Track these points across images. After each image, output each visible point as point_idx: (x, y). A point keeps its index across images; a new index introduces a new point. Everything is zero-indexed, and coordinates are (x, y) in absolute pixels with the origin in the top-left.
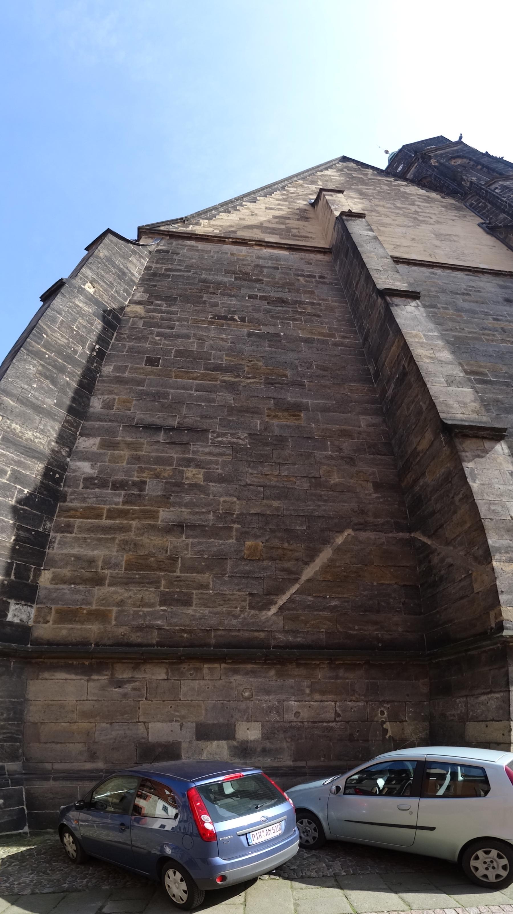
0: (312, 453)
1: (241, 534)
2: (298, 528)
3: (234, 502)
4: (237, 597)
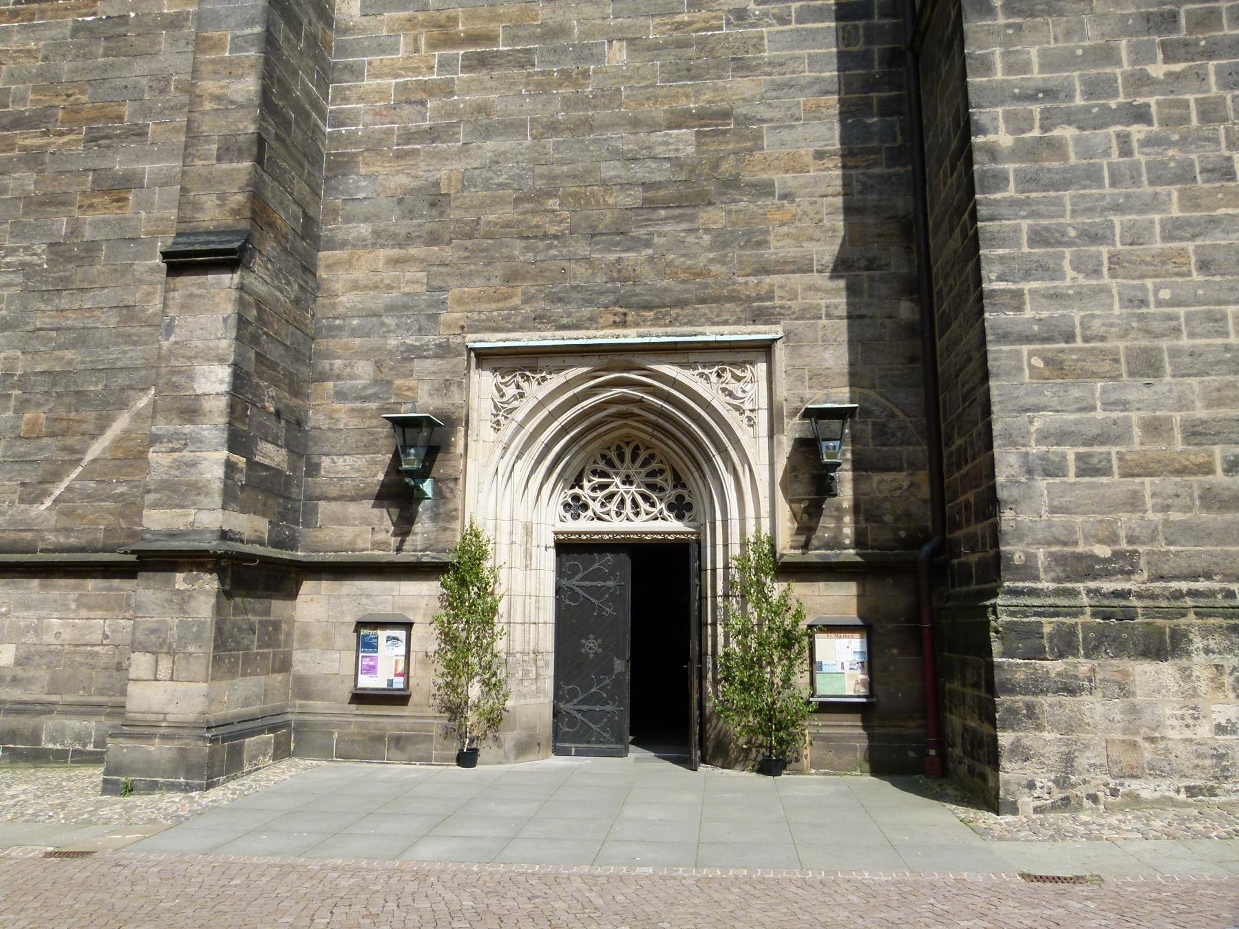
0: (131, 265)
1: (22, 402)
2: (92, 388)
3: (17, 358)
4: (6, 488)
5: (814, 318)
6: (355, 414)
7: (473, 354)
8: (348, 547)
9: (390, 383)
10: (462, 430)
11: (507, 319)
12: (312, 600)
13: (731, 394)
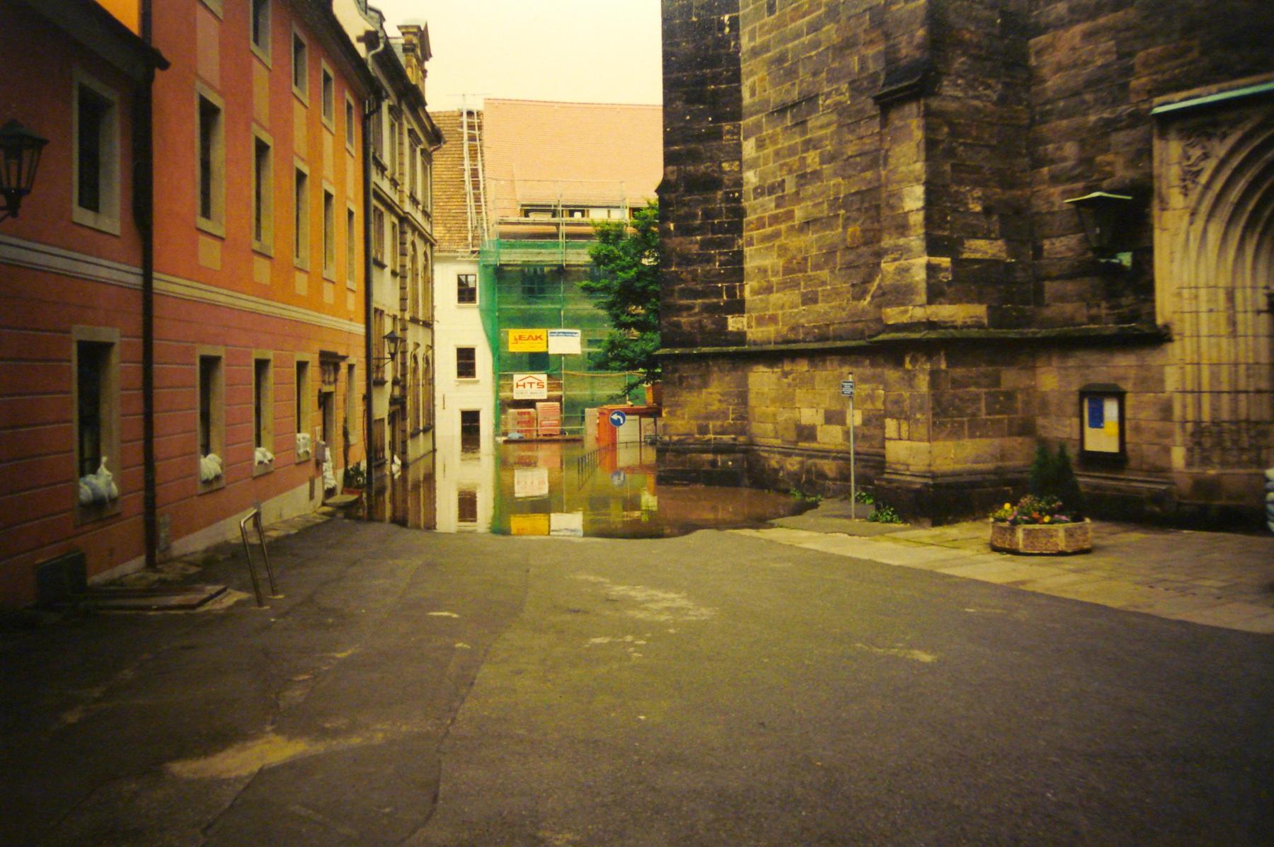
3: (840, 185)
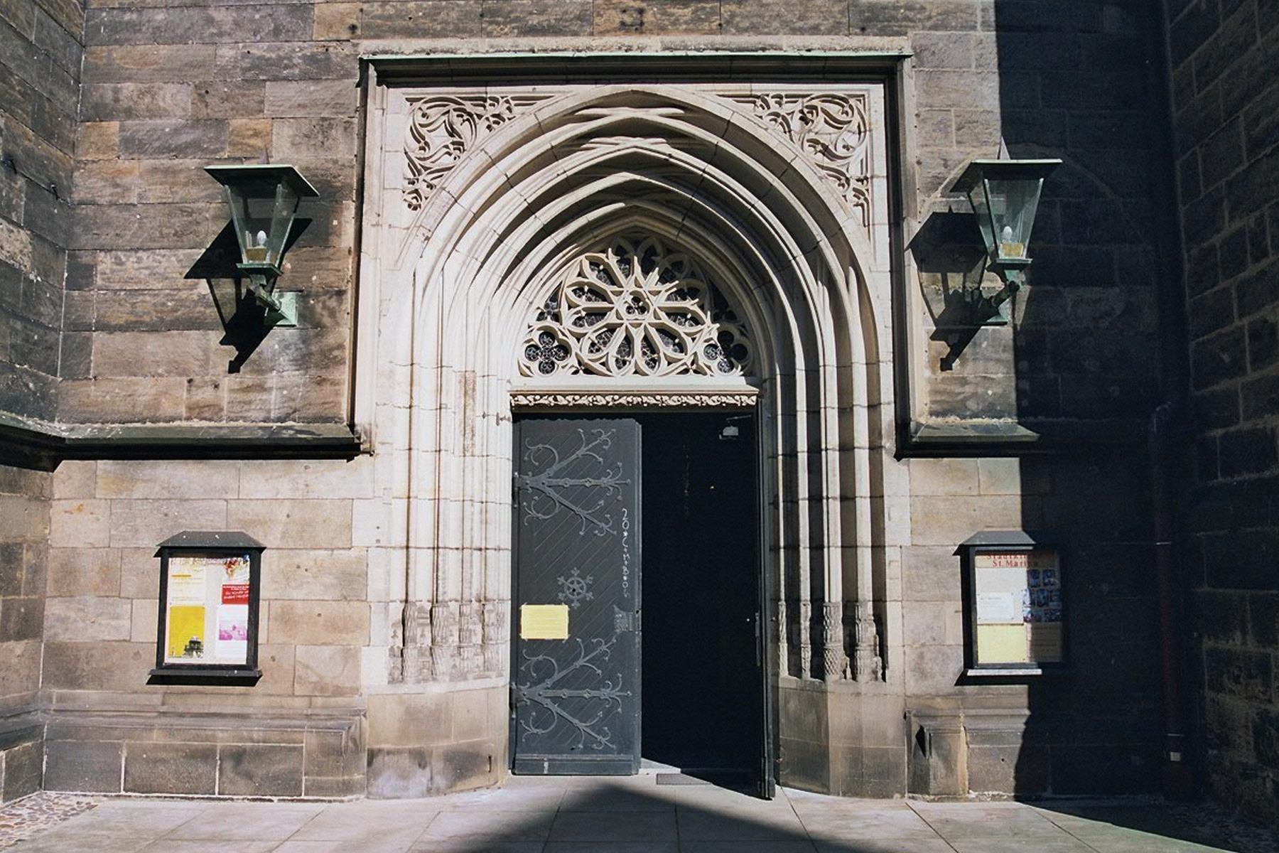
5: (963, 28)
6: (158, 177)
7: (372, 72)
8: (145, 414)
9: (220, 123)
10: (350, 208)
11: (432, 14)
12: (79, 509)
13: (826, 151)
